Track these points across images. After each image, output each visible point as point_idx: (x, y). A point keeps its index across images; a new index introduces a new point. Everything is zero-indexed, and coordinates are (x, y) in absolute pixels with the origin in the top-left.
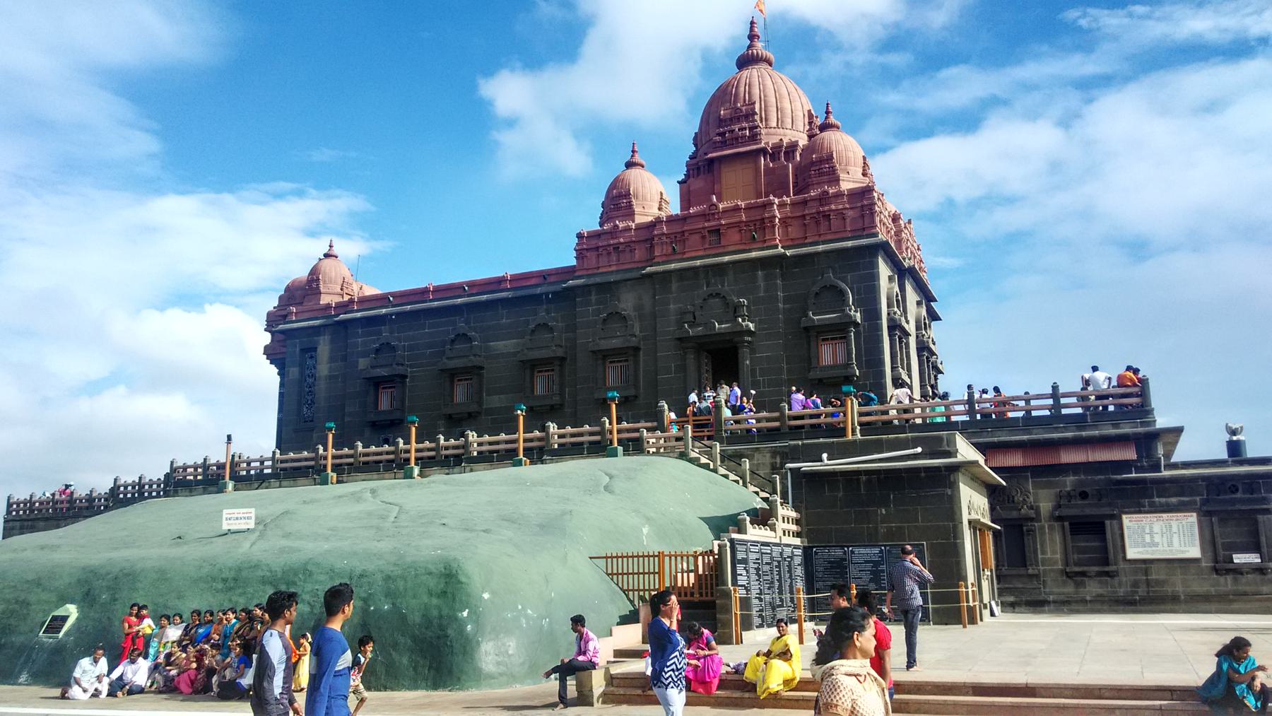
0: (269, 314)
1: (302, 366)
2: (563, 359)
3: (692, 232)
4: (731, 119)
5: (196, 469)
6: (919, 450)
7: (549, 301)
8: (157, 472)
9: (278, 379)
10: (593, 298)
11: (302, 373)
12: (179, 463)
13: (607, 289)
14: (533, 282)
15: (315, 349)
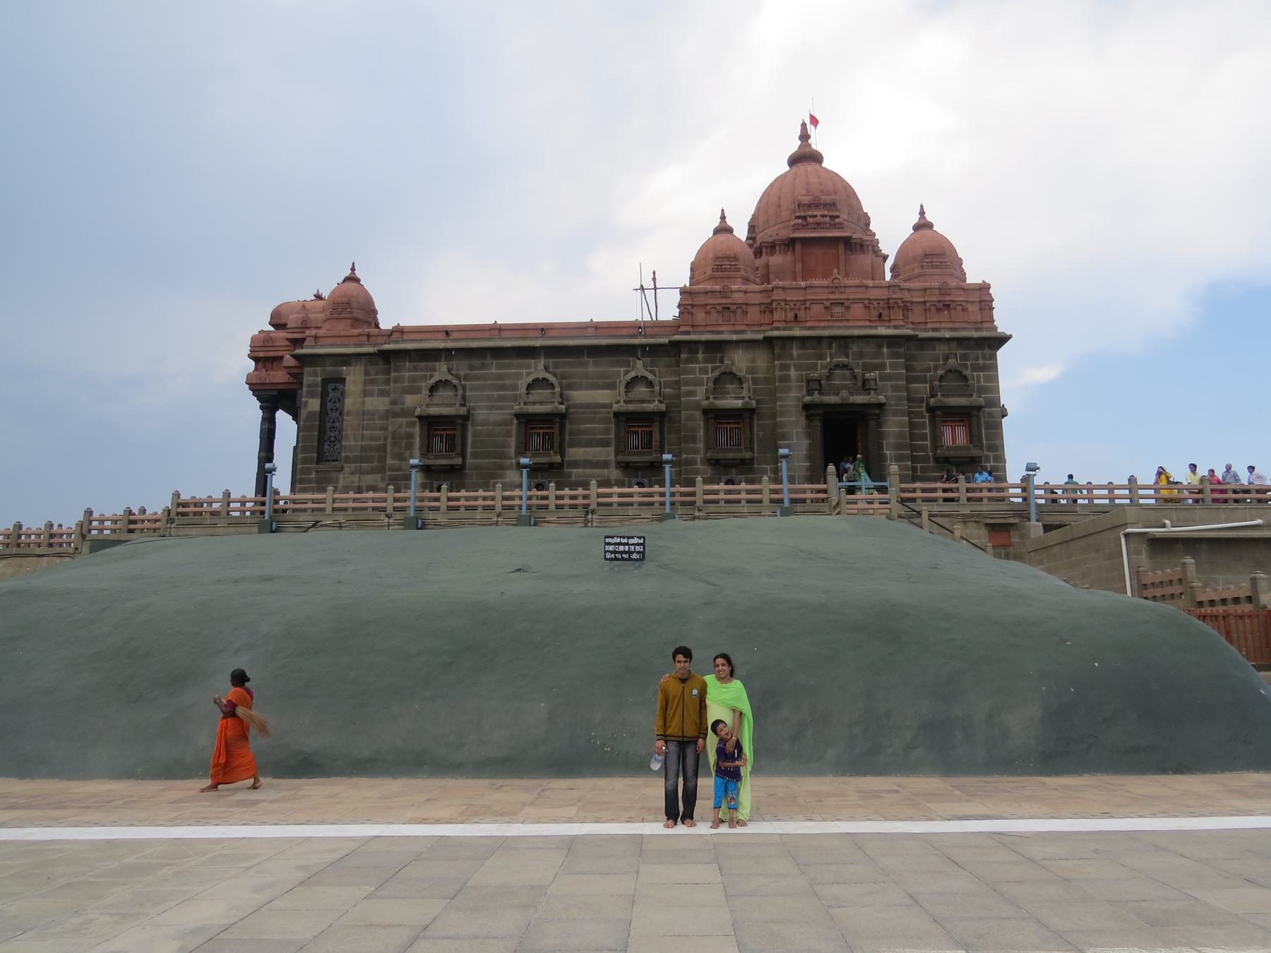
0: (253, 339)
1: (324, 397)
2: (662, 415)
3: (815, 302)
4: (809, 206)
5: (243, 503)
6: (1259, 521)
7: (645, 354)
8: (157, 504)
9: (260, 413)
10: (700, 356)
11: (323, 405)
12: (185, 497)
13: (716, 348)
14: (625, 332)
15: (343, 381)
